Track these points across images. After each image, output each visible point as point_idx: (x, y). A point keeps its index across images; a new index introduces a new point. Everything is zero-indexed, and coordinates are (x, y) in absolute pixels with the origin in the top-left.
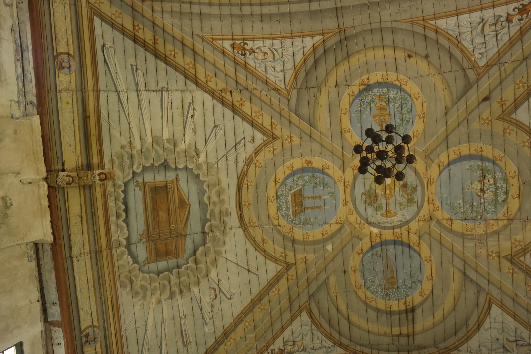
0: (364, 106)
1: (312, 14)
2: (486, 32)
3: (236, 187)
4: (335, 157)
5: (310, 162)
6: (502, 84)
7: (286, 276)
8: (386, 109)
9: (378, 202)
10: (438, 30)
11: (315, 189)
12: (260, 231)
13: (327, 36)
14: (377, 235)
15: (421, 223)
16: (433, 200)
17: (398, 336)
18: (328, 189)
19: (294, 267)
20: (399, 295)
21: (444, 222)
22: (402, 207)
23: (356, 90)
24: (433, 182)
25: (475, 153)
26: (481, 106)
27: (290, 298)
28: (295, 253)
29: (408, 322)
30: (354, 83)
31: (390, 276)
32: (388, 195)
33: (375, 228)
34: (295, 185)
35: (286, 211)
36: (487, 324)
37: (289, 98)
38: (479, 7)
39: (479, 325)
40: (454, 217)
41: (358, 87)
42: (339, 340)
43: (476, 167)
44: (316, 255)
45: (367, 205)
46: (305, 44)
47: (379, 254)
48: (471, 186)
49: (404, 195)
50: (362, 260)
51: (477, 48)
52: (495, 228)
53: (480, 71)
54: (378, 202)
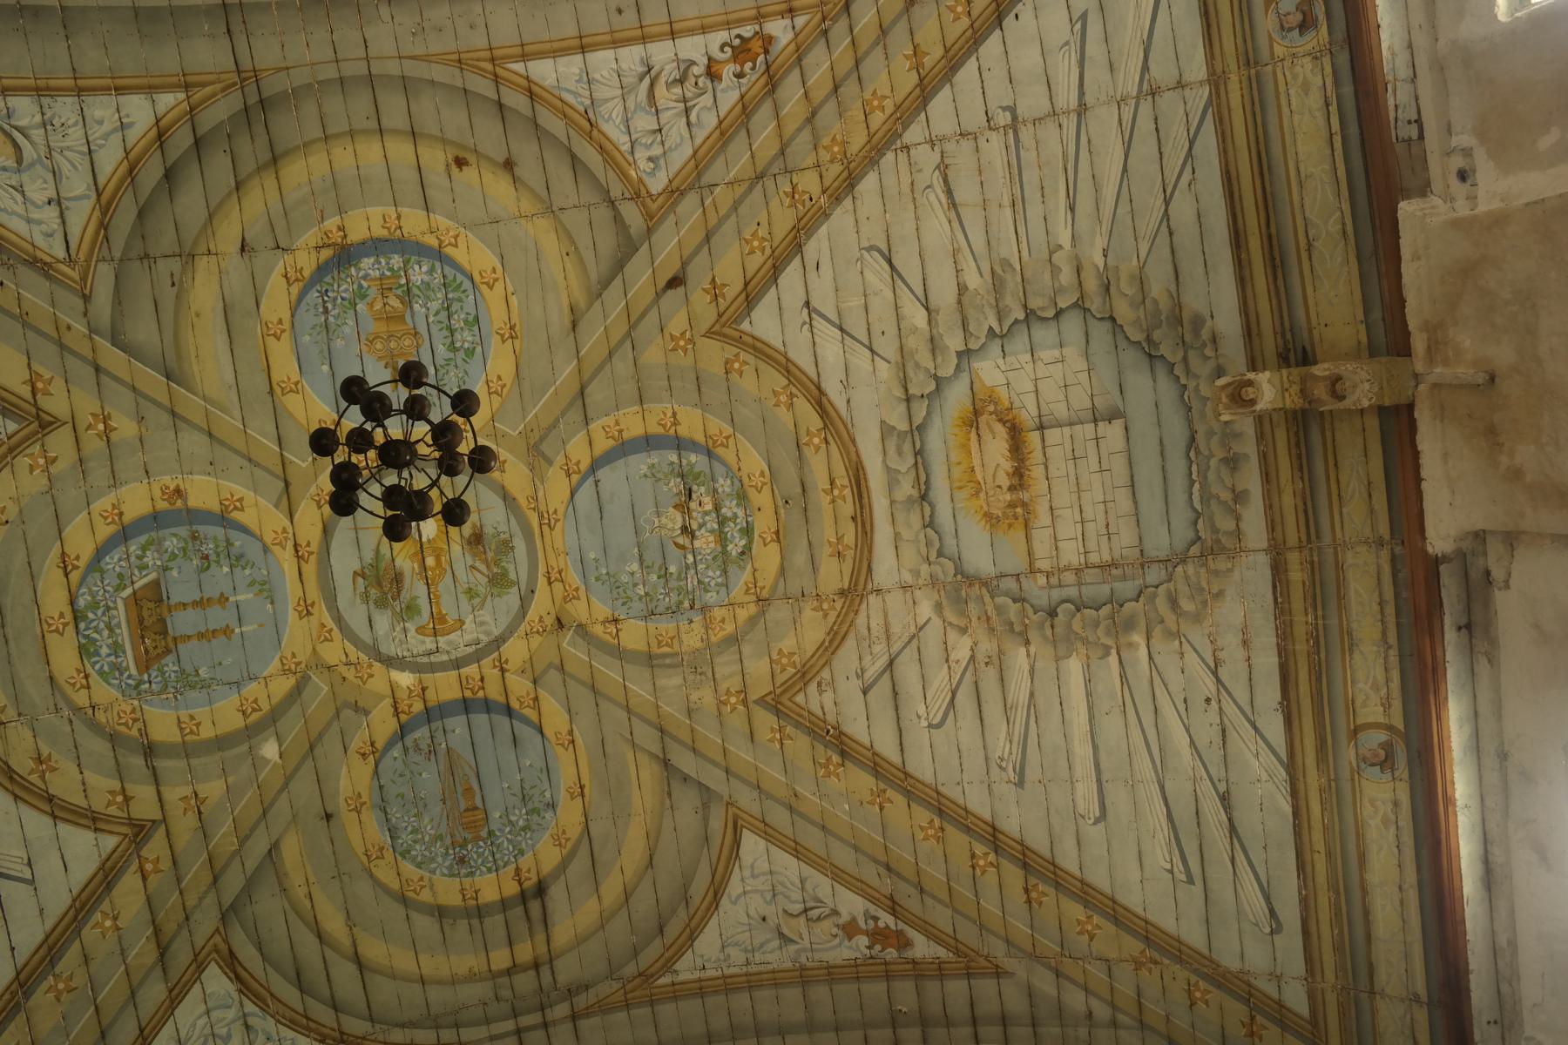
0: (337, 311)
2: (661, 103)
4: (259, 472)
5: (178, 492)
6: (712, 241)
7: (135, 866)
8: (401, 319)
9: (405, 595)
10: (535, 89)
11: (203, 576)
12: (28, 734)
13: (199, 95)
14: (411, 691)
15: (536, 641)
17: (509, 972)
18: (247, 572)
19: (161, 832)
20: (498, 856)
21: (598, 629)
22: (477, 601)
23: (307, 262)
24: (557, 521)
25: (660, 430)
27: (157, 931)
28: (157, 784)
29: (530, 929)
30: (300, 243)
31: (463, 806)
32: (433, 570)
33: (404, 671)
34: (136, 572)
36: (735, 886)
37: (87, 292)
38: (639, 32)
39: (716, 894)
41: (314, 253)
42: (335, 1026)
43: (666, 469)
44: (230, 780)
46: (128, 116)
47: (424, 746)
48: (656, 520)
49: (478, 564)
50: (376, 772)
51: (641, 144)
52: (729, 628)
53: (654, 206)
54: (403, 594)
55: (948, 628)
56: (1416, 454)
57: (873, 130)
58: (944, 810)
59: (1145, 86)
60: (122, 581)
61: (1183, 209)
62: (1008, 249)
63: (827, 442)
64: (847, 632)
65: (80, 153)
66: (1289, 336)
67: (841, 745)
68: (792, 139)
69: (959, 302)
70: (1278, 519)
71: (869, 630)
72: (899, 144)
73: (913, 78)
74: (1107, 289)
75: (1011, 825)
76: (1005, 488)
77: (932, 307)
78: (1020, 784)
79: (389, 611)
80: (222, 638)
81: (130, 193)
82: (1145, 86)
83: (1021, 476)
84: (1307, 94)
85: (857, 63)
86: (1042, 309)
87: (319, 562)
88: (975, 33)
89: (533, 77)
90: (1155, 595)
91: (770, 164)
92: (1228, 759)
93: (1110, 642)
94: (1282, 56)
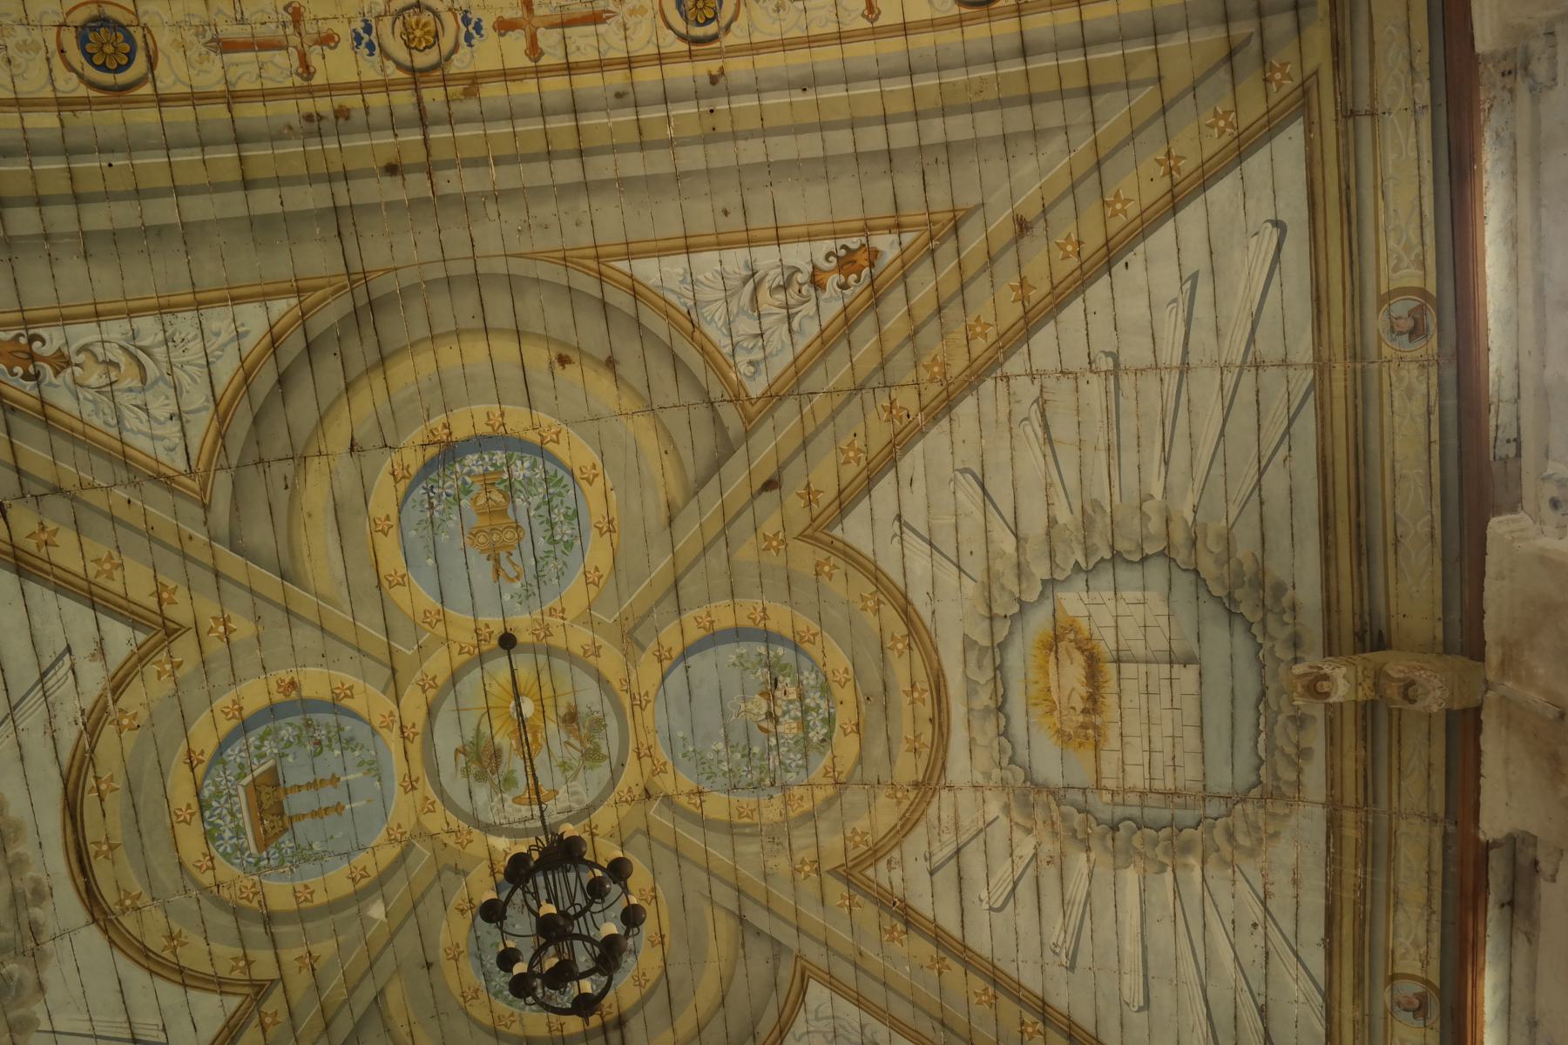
1: (258, 227)
2: (764, 308)
3: (60, 806)
5: (293, 684)
6: (809, 448)
8: (504, 513)
9: (503, 769)
10: (638, 288)
12: (160, 915)
15: (624, 810)
16: (649, 749)
18: (357, 753)
19: (278, 992)
22: (570, 773)
23: (413, 460)
24: (648, 702)
25: (749, 623)
26: (757, 502)
28: (275, 947)
33: (500, 836)
34: (255, 761)
35: (235, 840)
37: (206, 501)
39: (781, 1032)
40: (705, 786)
41: (419, 450)
43: (754, 659)
44: (340, 939)
45: (472, 779)
46: (243, 325)
49: (572, 741)
51: (743, 348)
52: (807, 806)
53: (752, 410)
54: (502, 767)
55: (1014, 828)
56: (1478, 752)
57: (974, 356)
58: (997, 980)
59: (1250, 358)
60: (242, 770)
61: (1276, 483)
62: (1100, 491)
63: (910, 648)
64: (918, 820)
65: (200, 366)
66: (1367, 618)
67: (907, 916)
68: (893, 354)
69: (1048, 534)
70: (1337, 780)
71: (939, 820)
72: (999, 372)
73: (1018, 310)
74: (1194, 543)
75: (1060, 1000)
76: (1079, 711)
77: (1021, 535)
78: (1072, 968)
79: (488, 784)
80: (334, 815)
81: (245, 402)
82: (1250, 358)
83: (1095, 702)
84: (1410, 399)
85: (963, 287)
86: (1129, 552)
87: (424, 743)
88: (1083, 274)
89: (637, 276)
90: (1214, 826)
91: (869, 377)
92: (1269, 978)
93: (1167, 860)
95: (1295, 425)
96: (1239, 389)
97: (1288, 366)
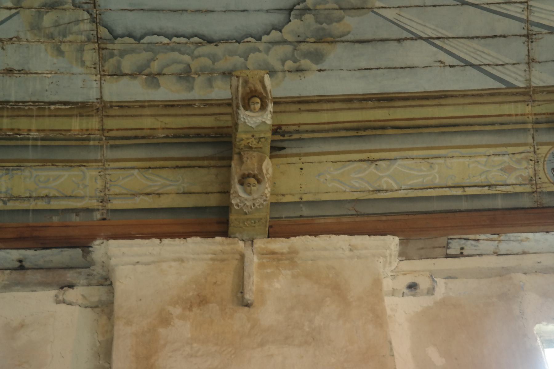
56: (185, 235)
59: (536, 29)
66: (295, 136)
82: (536, 29)
84: (501, 170)
94: (538, 152)
95: (475, 72)
96: (507, 20)
97: (528, 63)
